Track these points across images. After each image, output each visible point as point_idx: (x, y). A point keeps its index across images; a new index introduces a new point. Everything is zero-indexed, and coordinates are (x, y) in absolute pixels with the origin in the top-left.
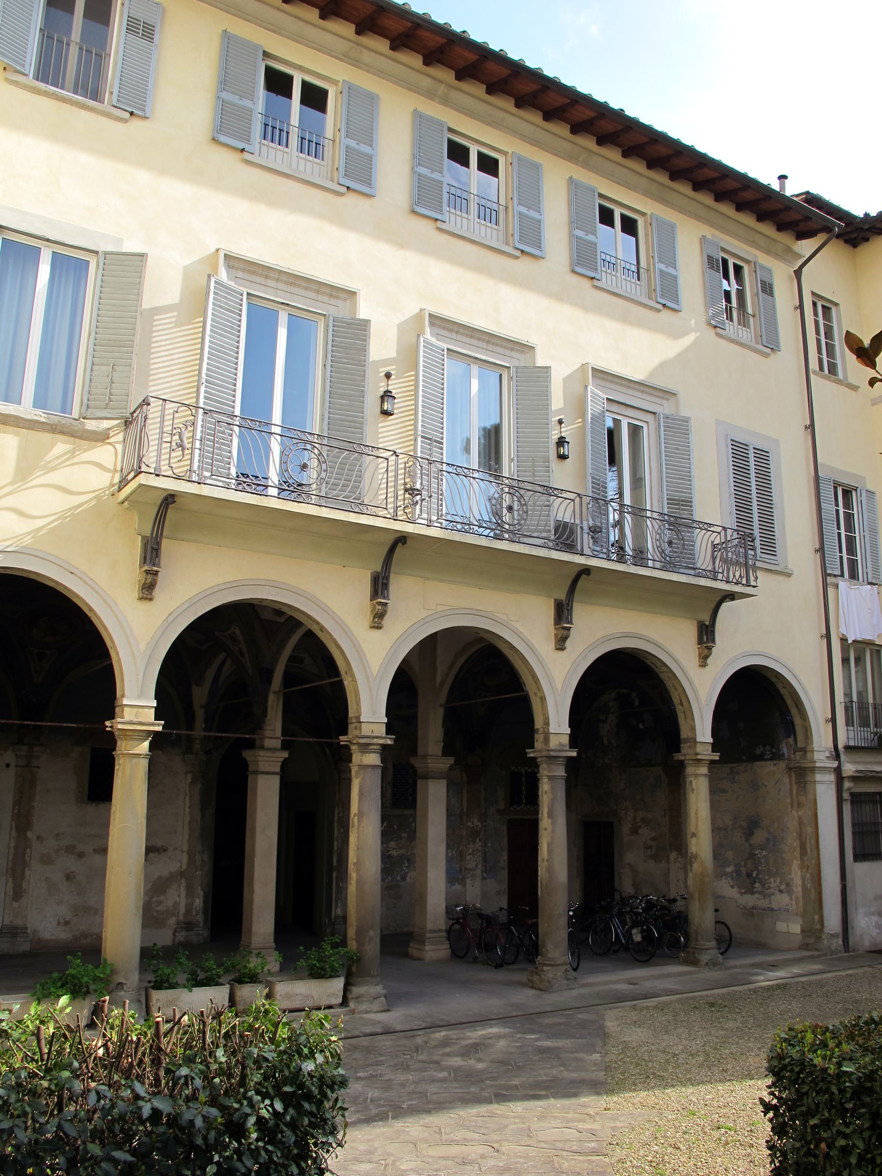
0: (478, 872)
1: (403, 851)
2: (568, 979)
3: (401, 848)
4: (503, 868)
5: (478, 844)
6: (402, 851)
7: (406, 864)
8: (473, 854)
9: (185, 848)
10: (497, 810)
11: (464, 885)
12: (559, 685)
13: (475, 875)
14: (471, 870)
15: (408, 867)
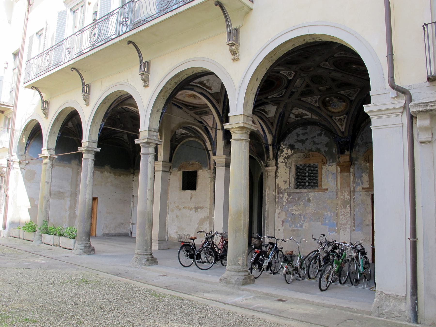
0: (348, 226)
1: (301, 212)
2: (136, 262)
3: (299, 210)
4: (368, 225)
5: (348, 209)
6: (300, 211)
7: (303, 219)
8: (344, 215)
9: (209, 208)
10: (363, 189)
11: (339, 234)
12: (145, 105)
13: (346, 228)
14: (344, 224)
15: (304, 220)
